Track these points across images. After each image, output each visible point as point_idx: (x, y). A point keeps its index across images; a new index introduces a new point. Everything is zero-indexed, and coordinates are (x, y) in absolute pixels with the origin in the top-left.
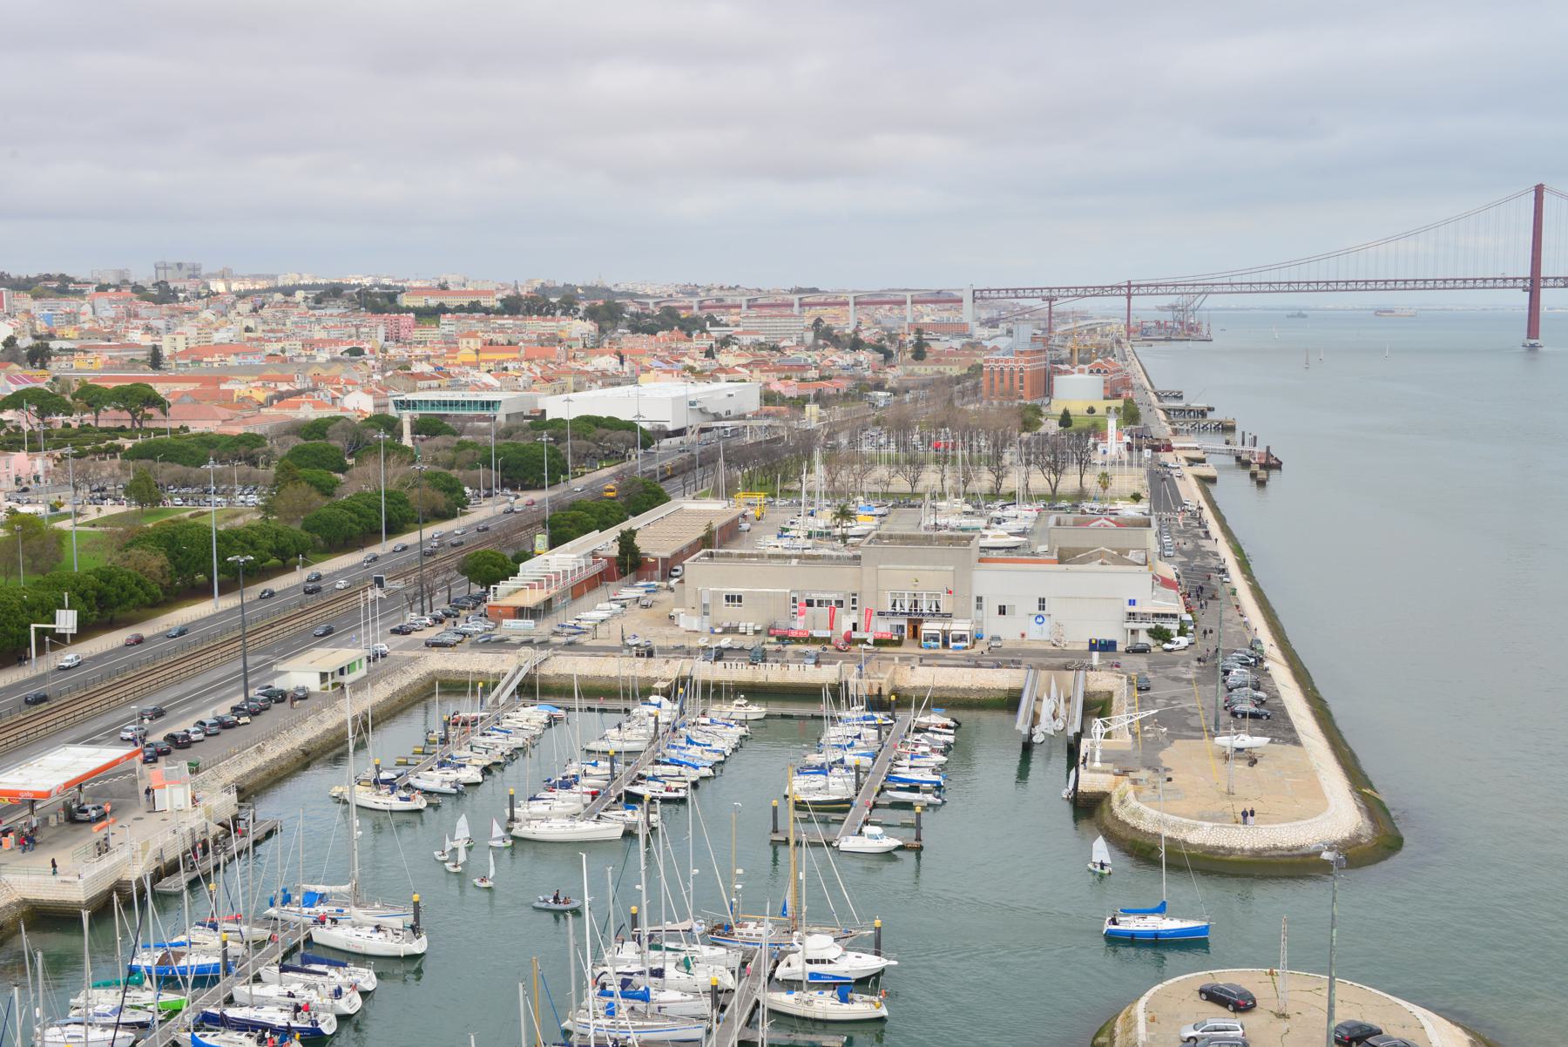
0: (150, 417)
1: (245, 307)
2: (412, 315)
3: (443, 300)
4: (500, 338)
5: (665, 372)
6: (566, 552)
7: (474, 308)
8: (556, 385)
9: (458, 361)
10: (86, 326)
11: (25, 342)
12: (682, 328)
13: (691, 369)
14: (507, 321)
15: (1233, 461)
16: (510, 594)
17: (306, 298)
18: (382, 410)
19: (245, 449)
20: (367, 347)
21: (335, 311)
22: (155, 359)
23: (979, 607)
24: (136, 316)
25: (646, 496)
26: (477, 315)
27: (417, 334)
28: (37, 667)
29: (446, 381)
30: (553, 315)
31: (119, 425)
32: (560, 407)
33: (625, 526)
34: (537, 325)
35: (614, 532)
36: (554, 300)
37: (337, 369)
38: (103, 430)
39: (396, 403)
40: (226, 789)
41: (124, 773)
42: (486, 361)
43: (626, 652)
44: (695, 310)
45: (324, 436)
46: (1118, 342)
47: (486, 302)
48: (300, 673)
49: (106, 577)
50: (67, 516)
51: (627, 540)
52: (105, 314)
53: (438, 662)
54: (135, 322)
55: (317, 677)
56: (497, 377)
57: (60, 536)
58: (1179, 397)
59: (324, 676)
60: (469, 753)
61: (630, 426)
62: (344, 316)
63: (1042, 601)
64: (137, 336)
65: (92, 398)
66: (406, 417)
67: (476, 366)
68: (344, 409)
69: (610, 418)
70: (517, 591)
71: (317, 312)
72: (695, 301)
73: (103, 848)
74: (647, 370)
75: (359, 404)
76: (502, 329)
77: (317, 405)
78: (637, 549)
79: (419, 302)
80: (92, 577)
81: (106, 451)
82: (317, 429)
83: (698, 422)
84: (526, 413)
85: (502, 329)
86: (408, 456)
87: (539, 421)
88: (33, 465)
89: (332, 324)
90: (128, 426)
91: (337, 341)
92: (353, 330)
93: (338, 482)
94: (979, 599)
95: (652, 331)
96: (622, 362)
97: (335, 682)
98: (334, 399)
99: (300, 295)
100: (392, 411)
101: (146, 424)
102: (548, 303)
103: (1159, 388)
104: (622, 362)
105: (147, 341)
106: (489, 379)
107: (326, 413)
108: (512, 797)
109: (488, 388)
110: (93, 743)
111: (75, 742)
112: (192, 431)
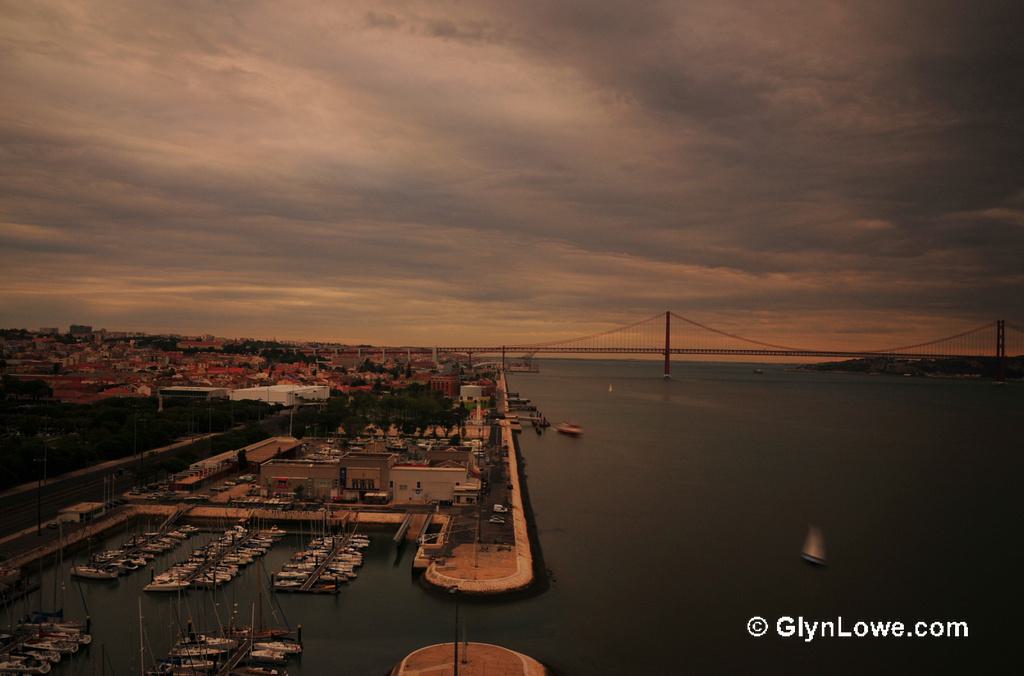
1: (105, 347)
7: (211, 349)
13: (302, 380)
14: (226, 356)
15: (530, 423)
21: (146, 349)
23: (391, 486)
32: (238, 395)
35: (235, 453)
46: (499, 373)
48: (73, 513)
51: (242, 455)
58: (517, 396)
63: (419, 483)
72: (314, 350)
75: (145, 390)
83: (297, 403)
94: (392, 483)
97: (87, 518)
99: (132, 342)
103: (510, 392)
107: (129, 395)
108: (152, 571)
109: (207, 385)
112: (63, 402)
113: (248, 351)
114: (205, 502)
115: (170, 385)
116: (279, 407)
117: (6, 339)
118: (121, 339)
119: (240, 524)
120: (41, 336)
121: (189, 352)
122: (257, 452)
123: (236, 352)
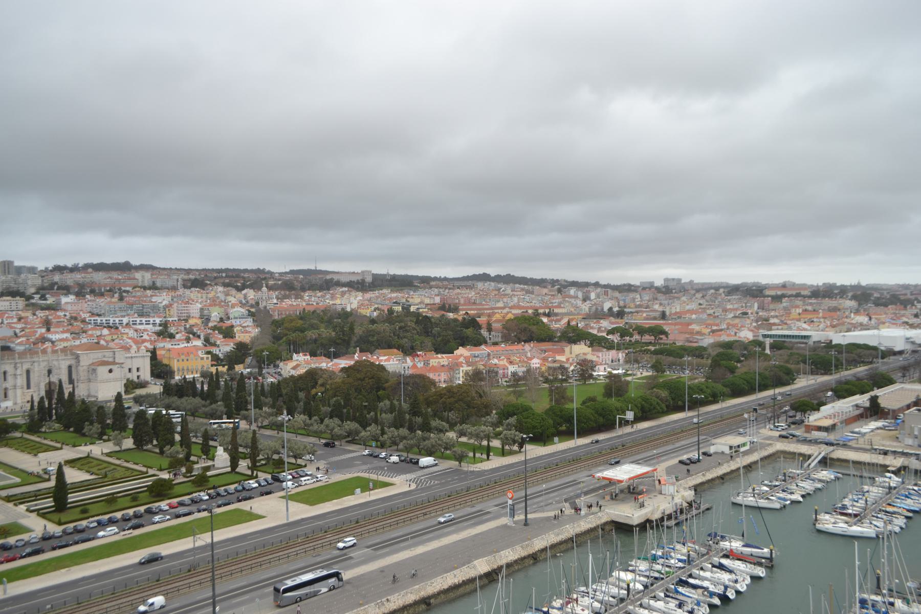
0: (661, 339)
2: (770, 298)
3: (785, 292)
4: (810, 308)
5: (893, 324)
6: (843, 403)
7: (798, 295)
8: (837, 329)
9: (790, 318)
10: (638, 303)
11: (616, 309)
12: (901, 304)
13: (907, 323)
14: (813, 301)
16: (815, 420)
17: (724, 292)
18: (756, 338)
19: (699, 352)
20: (750, 312)
21: (737, 297)
22: (663, 316)
24: (656, 299)
25: (883, 381)
26: (800, 298)
27: (772, 306)
28: (619, 432)
29: (785, 327)
30: (836, 298)
31: (649, 341)
32: (840, 338)
33: (872, 393)
34: (828, 303)
35: (866, 397)
36: (836, 292)
37: (737, 321)
38: (643, 343)
39: (763, 335)
40: (690, 488)
41: (650, 477)
42: (804, 318)
43: (873, 451)
44: (909, 296)
45: (731, 348)
47: (804, 293)
48: (722, 444)
49: (645, 399)
50: (630, 375)
51: (874, 400)
52: (645, 298)
53: (780, 446)
54: (656, 301)
55: (728, 448)
56: (809, 325)
57: (628, 383)
59: (731, 448)
60: (795, 487)
61: (875, 348)
62: (740, 299)
64: (657, 307)
65: (641, 331)
66: (768, 341)
67: (799, 320)
68: (739, 337)
69: (865, 345)
70: (820, 419)
71: (729, 297)
72: (908, 292)
73: (642, 506)
74: (884, 323)
75: (746, 335)
76: (811, 304)
77: (729, 335)
78: (879, 404)
79: (773, 293)
80: (639, 399)
81: (645, 351)
82: (729, 345)
83: (909, 347)
84: (823, 341)
85: (811, 304)
86: (767, 358)
87: (829, 345)
88: (618, 355)
89: (734, 304)
90: (653, 342)
91: (736, 309)
92: (744, 305)
93: (736, 367)
95: (886, 305)
96: (870, 319)
97: (735, 450)
98: (736, 333)
99: (721, 290)
100: (761, 339)
101: (660, 341)
102: (832, 293)
104: (870, 319)
105: (661, 309)
106: (805, 326)
107: (732, 339)
108: (816, 510)
110: (639, 464)
111: (632, 462)
112: (678, 344)
113: (836, 294)
114: (845, 446)
115: (771, 330)
116: (890, 353)
117: (620, 292)
118: (711, 288)
119: (889, 472)
120: (644, 289)
121: (777, 299)
122: (888, 396)
123: (824, 297)
